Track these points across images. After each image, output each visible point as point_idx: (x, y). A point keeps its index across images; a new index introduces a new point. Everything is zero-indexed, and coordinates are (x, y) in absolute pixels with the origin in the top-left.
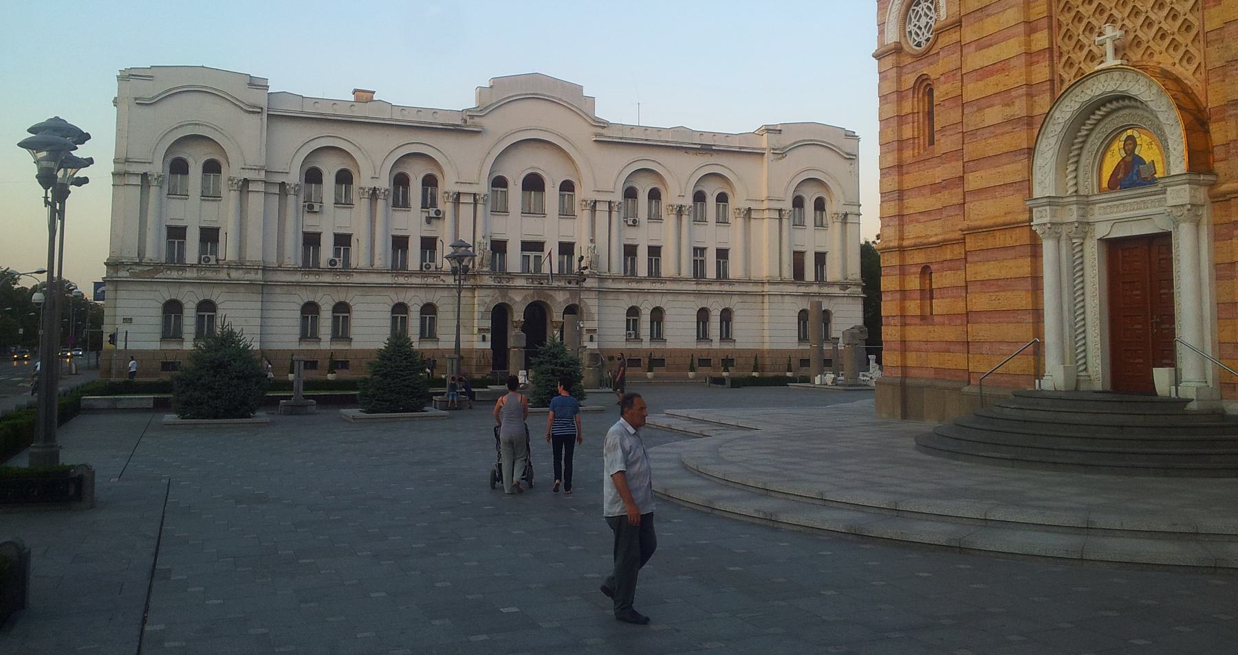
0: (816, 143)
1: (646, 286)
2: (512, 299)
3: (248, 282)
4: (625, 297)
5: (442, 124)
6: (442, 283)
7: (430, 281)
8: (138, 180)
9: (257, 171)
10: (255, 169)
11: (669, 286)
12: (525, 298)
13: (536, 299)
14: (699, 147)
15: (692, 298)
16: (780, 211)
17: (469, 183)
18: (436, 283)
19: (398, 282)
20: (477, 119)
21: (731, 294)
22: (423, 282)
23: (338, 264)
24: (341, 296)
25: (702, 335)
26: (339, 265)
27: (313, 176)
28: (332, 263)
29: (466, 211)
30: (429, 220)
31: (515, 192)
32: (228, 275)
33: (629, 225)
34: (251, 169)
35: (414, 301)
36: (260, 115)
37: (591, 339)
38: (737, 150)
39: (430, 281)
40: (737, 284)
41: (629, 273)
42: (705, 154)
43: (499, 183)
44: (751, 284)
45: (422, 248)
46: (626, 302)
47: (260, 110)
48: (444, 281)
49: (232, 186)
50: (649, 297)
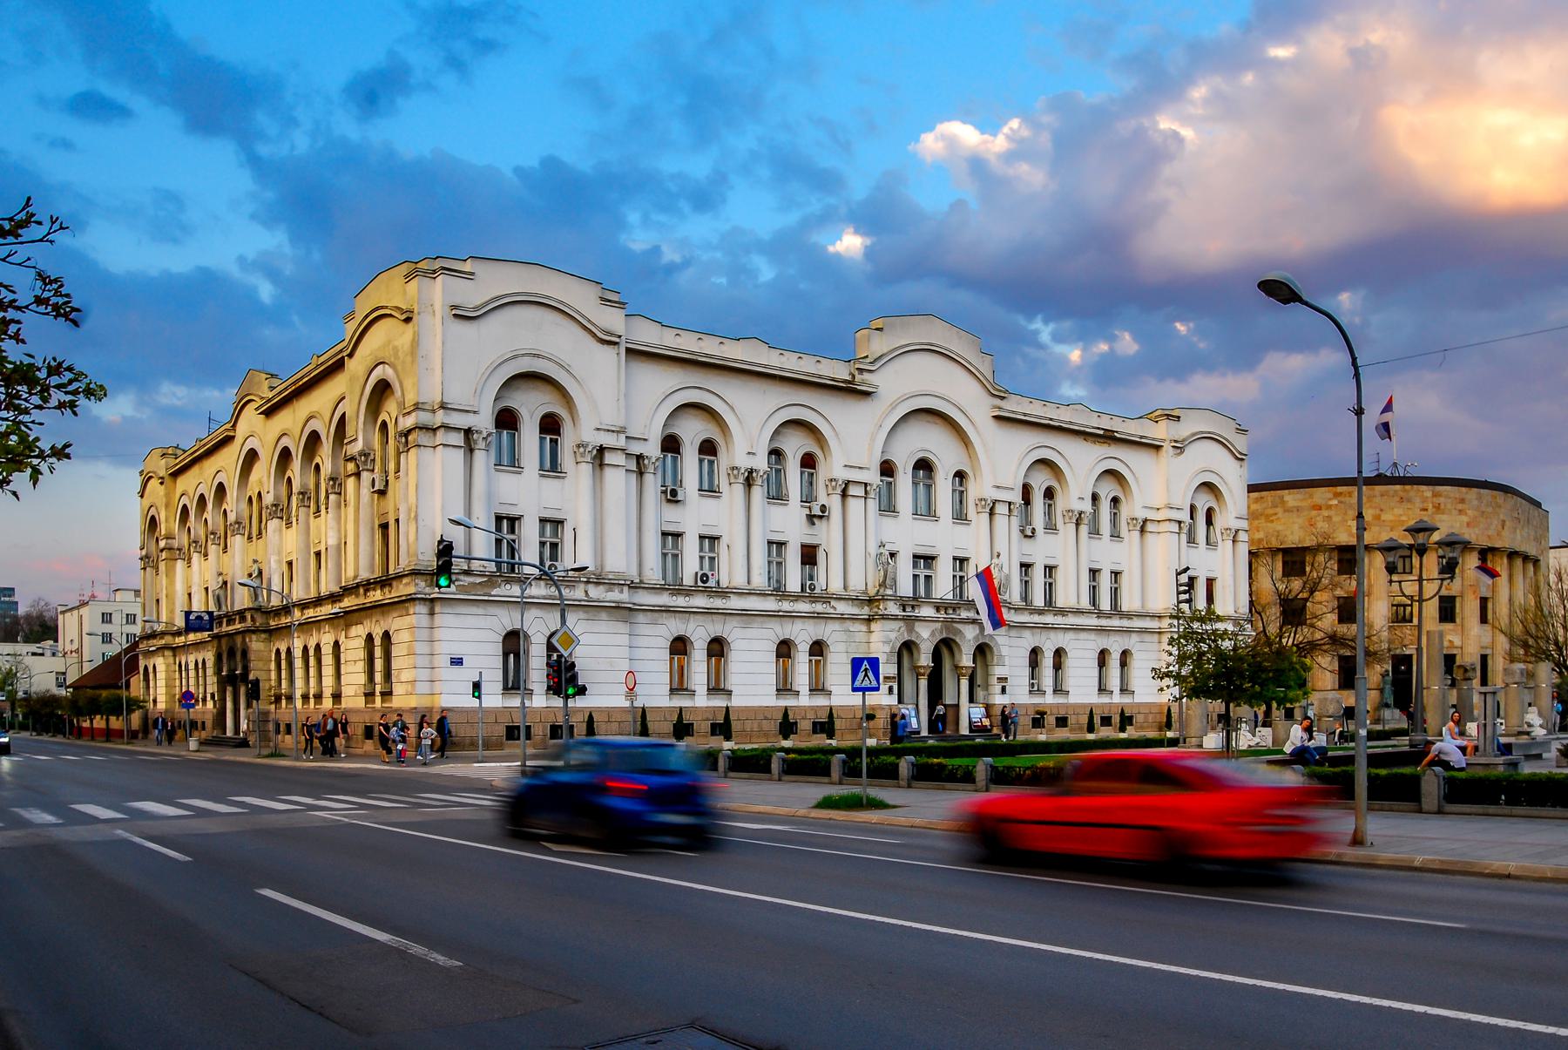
0: (1219, 438)
2: (918, 636)
3: (613, 605)
4: (1027, 634)
5: (833, 379)
6: (832, 611)
7: (819, 607)
8: (458, 439)
9: (615, 434)
10: (613, 431)
13: (944, 636)
14: (1101, 432)
15: (1092, 636)
17: (860, 468)
18: (826, 611)
20: (866, 376)
21: (1129, 631)
22: (812, 610)
23: (710, 580)
24: (716, 628)
29: (855, 506)
30: (811, 518)
31: (904, 481)
32: (586, 592)
33: (1026, 536)
34: (608, 431)
35: (803, 635)
36: (616, 347)
37: (1004, 690)
38: (1138, 440)
39: (819, 607)
40: (1135, 618)
42: (1104, 443)
43: (887, 469)
44: (1148, 618)
46: (1028, 640)
47: (617, 340)
48: (835, 609)
49: (583, 455)
50: (1052, 634)
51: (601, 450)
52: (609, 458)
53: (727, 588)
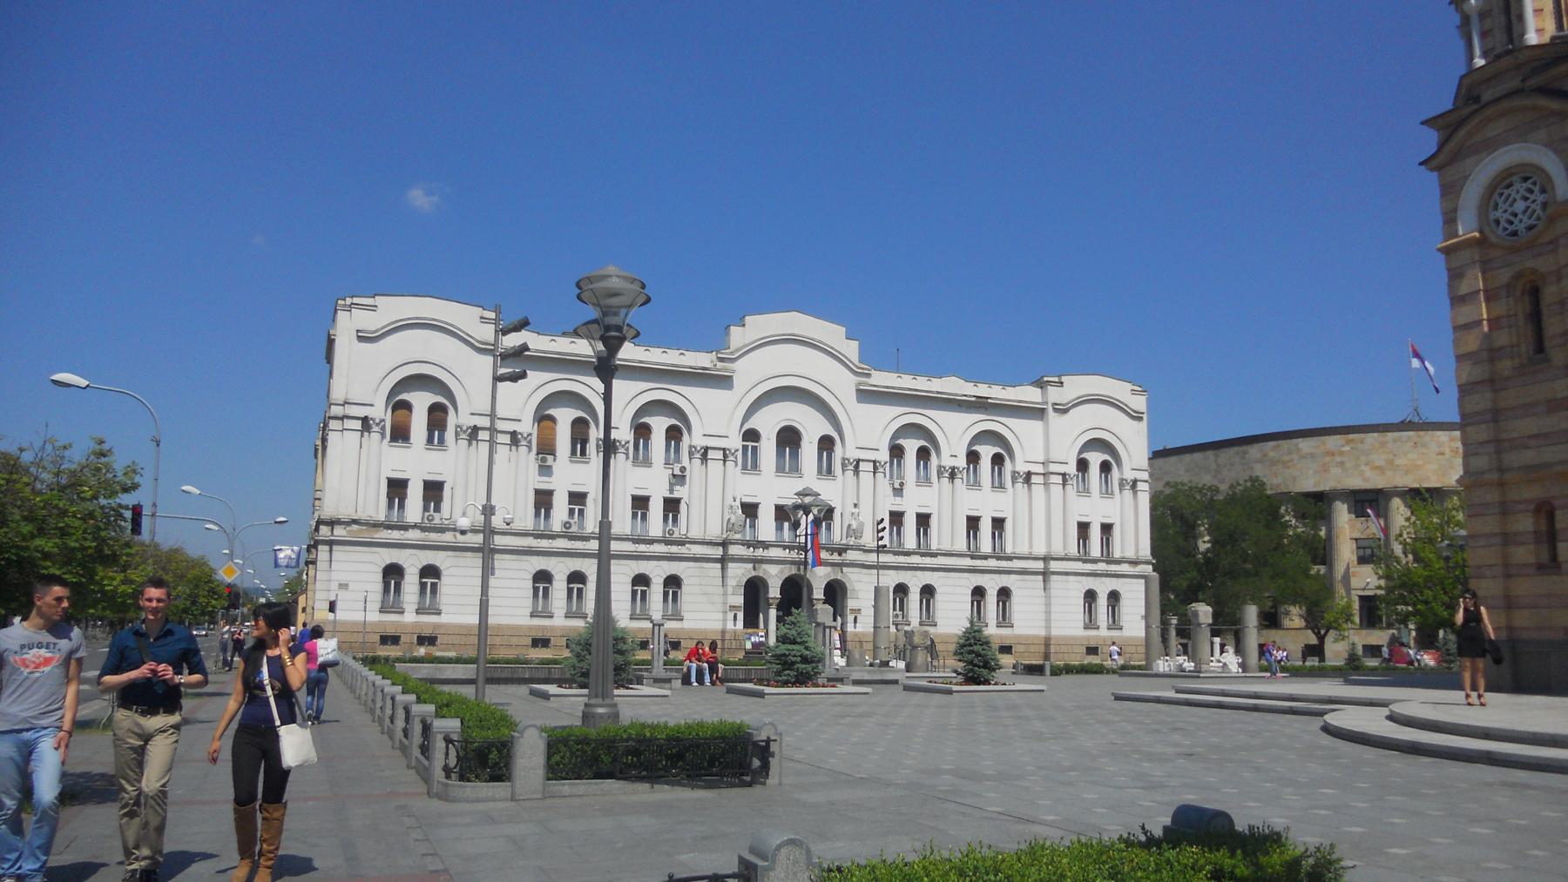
1: (916, 560)
2: (765, 571)
7: (674, 549)
11: (941, 561)
12: (782, 571)
16: (1064, 475)
19: (638, 550)
25: (1090, 623)
26: (574, 529)
27: (642, 431)
28: (567, 525)
32: (455, 536)
41: (1105, 554)
45: (776, 519)
48: (689, 549)
51: (706, 449)
52: (711, 454)
53: (592, 533)
